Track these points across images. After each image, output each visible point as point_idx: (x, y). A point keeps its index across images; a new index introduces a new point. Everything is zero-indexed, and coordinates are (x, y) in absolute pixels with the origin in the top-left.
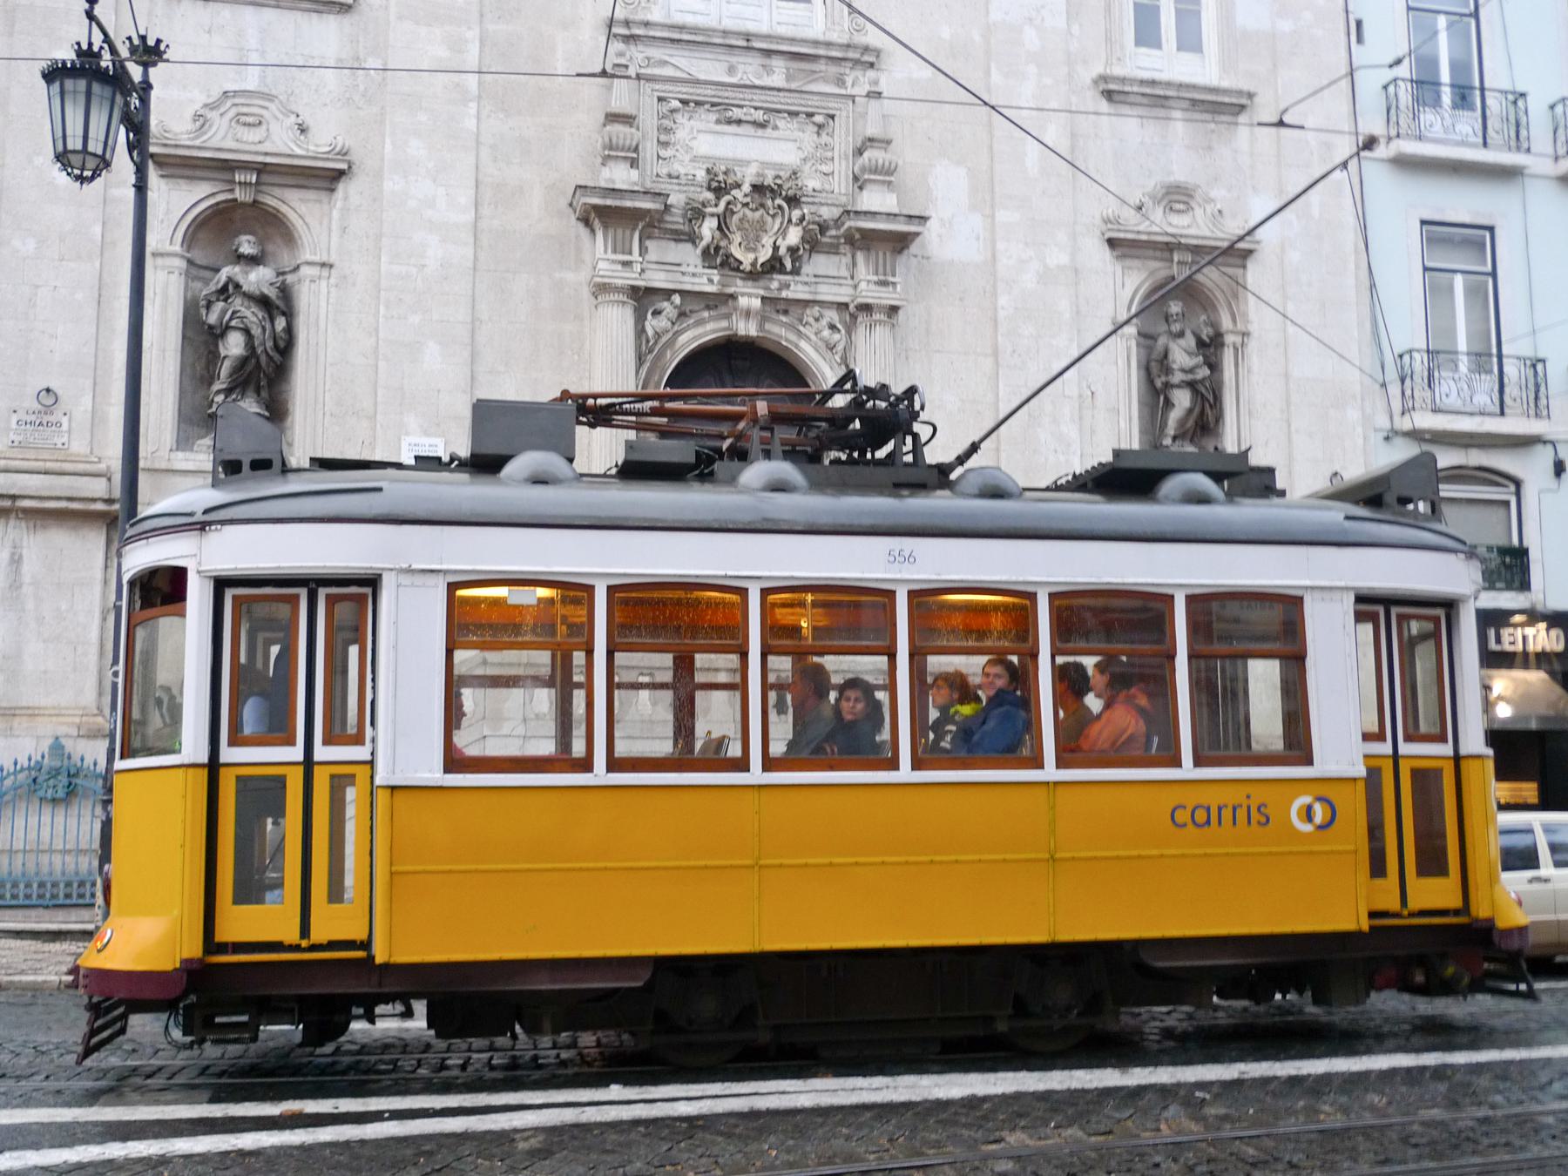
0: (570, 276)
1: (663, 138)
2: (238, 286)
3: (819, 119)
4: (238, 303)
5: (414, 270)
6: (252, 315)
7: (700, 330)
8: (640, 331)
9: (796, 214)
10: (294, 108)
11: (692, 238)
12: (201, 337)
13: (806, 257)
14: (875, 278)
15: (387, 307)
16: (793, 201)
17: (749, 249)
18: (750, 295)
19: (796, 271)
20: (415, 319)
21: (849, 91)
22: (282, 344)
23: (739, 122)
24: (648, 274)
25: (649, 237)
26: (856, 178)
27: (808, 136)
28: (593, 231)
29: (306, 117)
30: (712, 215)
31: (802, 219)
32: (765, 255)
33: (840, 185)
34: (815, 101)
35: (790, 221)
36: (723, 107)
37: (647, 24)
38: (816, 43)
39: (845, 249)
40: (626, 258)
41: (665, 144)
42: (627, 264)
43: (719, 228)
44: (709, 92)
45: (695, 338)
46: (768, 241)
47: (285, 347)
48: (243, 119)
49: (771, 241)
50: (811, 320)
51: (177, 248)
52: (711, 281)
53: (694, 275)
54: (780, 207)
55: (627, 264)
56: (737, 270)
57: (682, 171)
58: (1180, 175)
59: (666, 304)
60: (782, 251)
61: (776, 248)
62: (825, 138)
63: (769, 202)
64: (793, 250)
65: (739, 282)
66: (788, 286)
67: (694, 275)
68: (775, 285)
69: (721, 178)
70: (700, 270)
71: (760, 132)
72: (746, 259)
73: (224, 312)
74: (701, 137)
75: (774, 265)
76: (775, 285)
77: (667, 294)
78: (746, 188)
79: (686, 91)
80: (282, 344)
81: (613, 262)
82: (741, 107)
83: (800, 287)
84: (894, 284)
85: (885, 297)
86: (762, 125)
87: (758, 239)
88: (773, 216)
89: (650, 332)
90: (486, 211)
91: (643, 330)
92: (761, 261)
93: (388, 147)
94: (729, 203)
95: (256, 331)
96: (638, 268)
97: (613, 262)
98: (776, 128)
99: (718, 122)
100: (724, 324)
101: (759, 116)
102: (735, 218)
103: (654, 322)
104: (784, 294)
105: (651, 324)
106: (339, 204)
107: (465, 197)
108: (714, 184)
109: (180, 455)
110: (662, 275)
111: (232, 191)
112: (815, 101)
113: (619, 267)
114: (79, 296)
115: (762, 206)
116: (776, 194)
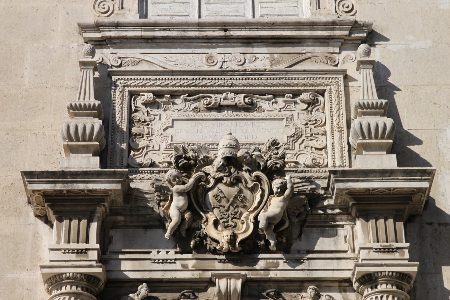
3: (306, 96)
9: (276, 183)
13: (296, 232)
14: (377, 245)
18: (229, 277)
21: (339, 67)
23: (219, 108)
25: (115, 226)
27: (299, 114)
28: (52, 226)
31: (283, 188)
32: (244, 231)
34: (301, 79)
35: (271, 192)
36: (196, 92)
37: (117, 26)
38: (299, 25)
40: (82, 246)
42: (84, 251)
44: (185, 82)
49: (252, 215)
53: (165, 261)
56: (215, 251)
60: (262, 223)
61: (256, 222)
62: (315, 115)
63: (246, 175)
67: (165, 261)
68: (261, 264)
69: (191, 154)
71: (243, 115)
72: (222, 236)
78: (218, 162)
79: (160, 83)
81: (66, 251)
87: (237, 216)
92: (241, 237)
94: (199, 179)
96: (94, 255)
97: (66, 251)
98: (261, 110)
99: (196, 110)
101: (240, 99)
104: (272, 274)
108: (182, 162)
112: (301, 79)
115: (237, 181)
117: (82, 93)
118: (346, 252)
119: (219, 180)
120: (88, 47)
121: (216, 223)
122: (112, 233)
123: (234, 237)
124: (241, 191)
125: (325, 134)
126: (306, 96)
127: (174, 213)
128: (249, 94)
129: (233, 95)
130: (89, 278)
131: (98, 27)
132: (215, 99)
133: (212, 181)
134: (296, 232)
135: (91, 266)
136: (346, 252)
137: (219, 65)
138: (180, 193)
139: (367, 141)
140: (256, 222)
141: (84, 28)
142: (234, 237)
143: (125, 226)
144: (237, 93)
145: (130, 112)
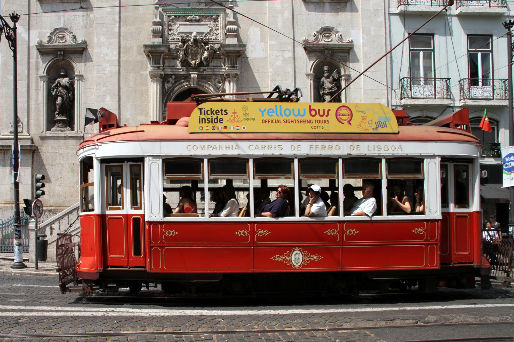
0: (144, 72)
1: (170, 28)
2: (60, 84)
4: (60, 89)
5: (103, 75)
6: (63, 91)
7: (180, 86)
8: (163, 87)
10: (72, 31)
11: (177, 58)
12: (51, 99)
15: (96, 85)
17: (194, 60)
19: (208, 65)
20: (104, 89)
22: (71, 99)
23: (191, 21)
24: (166, 70)
25: (166, 59)
26: (226, 34)
29: (75, 33)
32: (198, 61)
33: (221, 37)
39: (222, 57)
41: (170, 30)
43: (185, 54)
45: (179, 89)
46: (199, 57)
47: (72, 101)
48: (60, 36)
50: (213, 80)
51: (45, 74)
52: (183, 70)
54: (202, 46)
55: (159, 67)
57: (175, 37)
58: (328, 24)
59: (171, 79)
64: (206, 59)
65: (191, 70)
66: (205, 70)
70: (180, 67)
73: (57, 91)
74: (180, 26)
75: (201, 64)
76: (202, 70)
77: (171, 76)
80: (71, 99)
81: (155, 67)
82: (191, 16)
83: (209, 70)
84: (236, 67)
85: (235, 71)
87: (196, 56)
88: (200, 49)
89: (166, 88)
90: (121, 55)
91: (165, 87)
93: (96, 40)
95: (65, 96)
96: (162, 68)
99: (185, 21)
102: (189, 51)
103: (167, 85)
105: (167, 86)
106: (84, 58)
107: (116, 52)
109: (48, 132)
110: (169, 70)
111: (58, 57)
113: (157, 69)
114: (23, 90)
116: (200, 43)
122: (165, 60)
123: (195, 62)
125: (219, 29)
134: (211, 60)
140: (201, 58)
143: (169, 59)
145: (168, 22)
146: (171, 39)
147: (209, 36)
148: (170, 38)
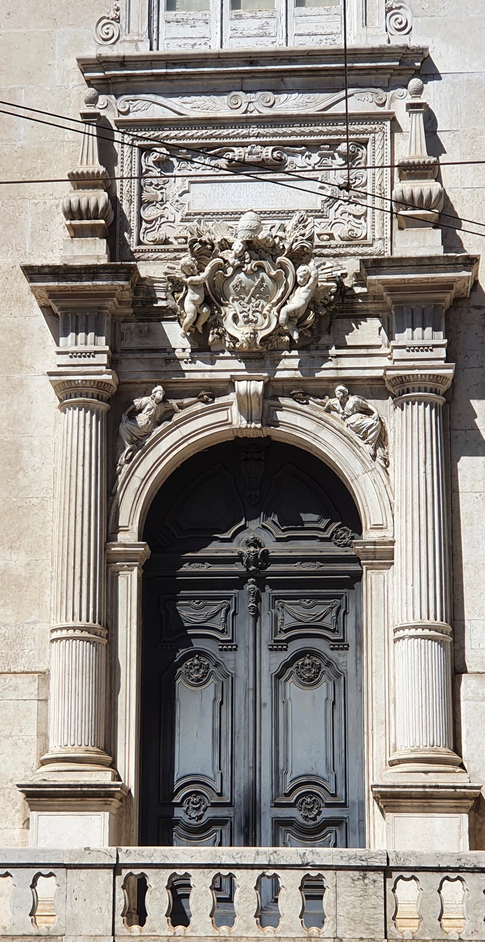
16: (300, 257)
30: (195, 286)
78: (238, 246)
86: (277, 166)
92: (261, 335)
100: (221, 416)
101: (267, 153)
117: (84, 156)
118: (379, 347)
119: (238, 269)
120: (92, 91)
121: (235, 318)
124: (263, 280)
126: (343, 147)
127: (189, 306)
128: (279, 146)
129: (259, 148)
130: (100, 384)
131: (103, 63)
132: (238, 153)
133: (230, 270)
135: (100, 373)
136: (379, 347)
137: (243, 108)
138: (195, 286)
139: (408, 213)
141: (85, 65)
142: (255, 333)
144: (264, 145)
146: (156, 242)
147: (319, 227)
148: (150, 237)
